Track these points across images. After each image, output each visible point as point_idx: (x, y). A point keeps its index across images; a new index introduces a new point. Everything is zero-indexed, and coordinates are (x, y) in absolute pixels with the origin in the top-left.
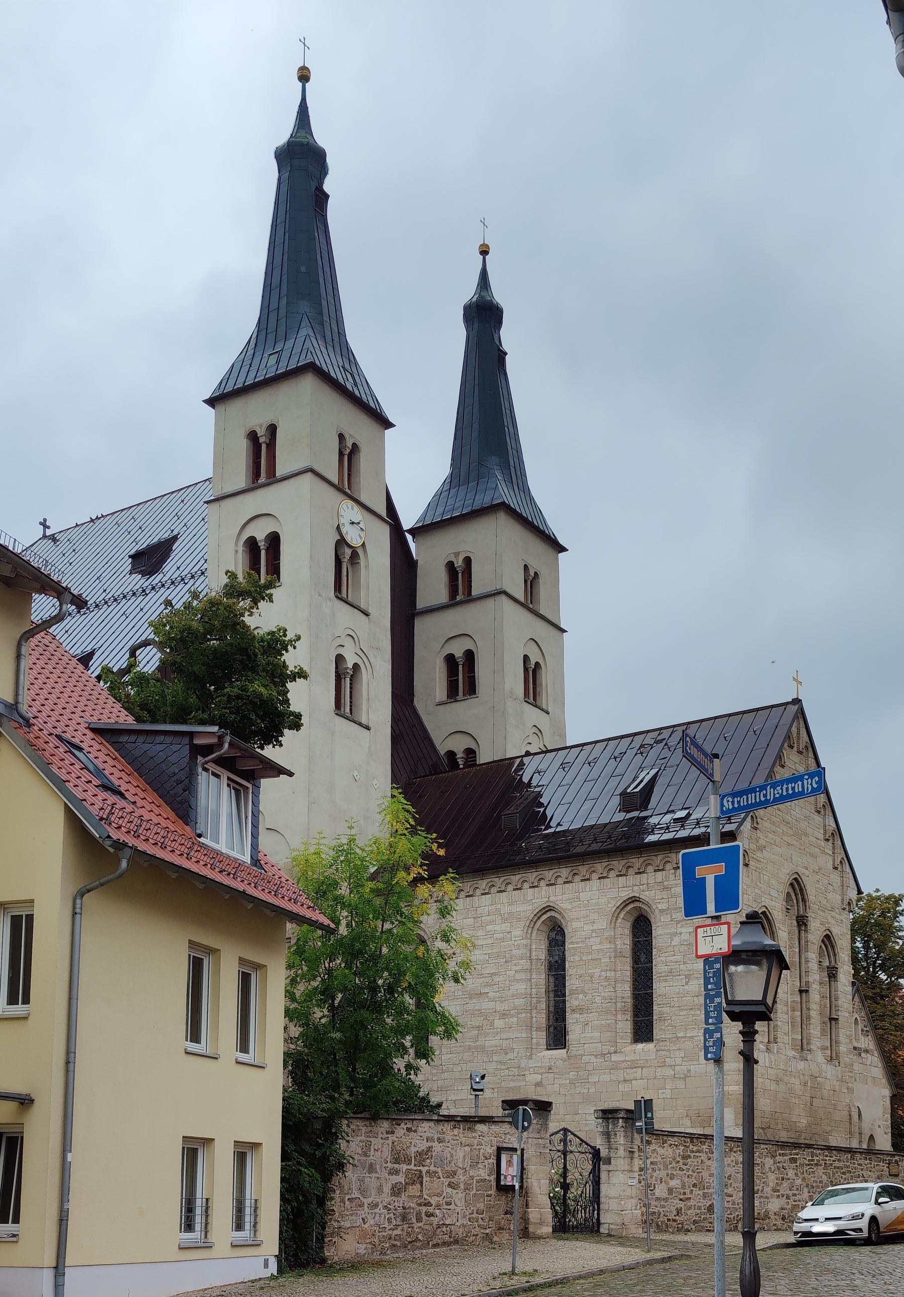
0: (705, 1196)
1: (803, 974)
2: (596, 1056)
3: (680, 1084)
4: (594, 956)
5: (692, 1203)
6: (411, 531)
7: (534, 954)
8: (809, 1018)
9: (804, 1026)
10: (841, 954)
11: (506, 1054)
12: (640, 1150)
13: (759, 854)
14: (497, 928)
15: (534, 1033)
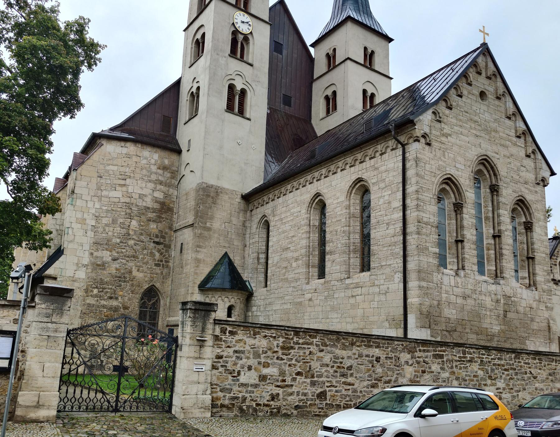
0: (313, 384)
1: (496, 225)
2: (338, 281)
3: (383, 298)
4: (338, 219)
5: (295, 389)
6: (313, 45)
7: (311, 222)
8: (501, 255)
9: (498, 261)
10: (536, 214)
11: (297, 282)
12: (216, 338)
13: (444, 139)
14: (295, 210)
15: (310, 269)
